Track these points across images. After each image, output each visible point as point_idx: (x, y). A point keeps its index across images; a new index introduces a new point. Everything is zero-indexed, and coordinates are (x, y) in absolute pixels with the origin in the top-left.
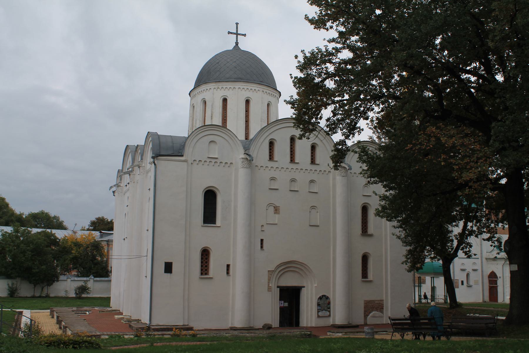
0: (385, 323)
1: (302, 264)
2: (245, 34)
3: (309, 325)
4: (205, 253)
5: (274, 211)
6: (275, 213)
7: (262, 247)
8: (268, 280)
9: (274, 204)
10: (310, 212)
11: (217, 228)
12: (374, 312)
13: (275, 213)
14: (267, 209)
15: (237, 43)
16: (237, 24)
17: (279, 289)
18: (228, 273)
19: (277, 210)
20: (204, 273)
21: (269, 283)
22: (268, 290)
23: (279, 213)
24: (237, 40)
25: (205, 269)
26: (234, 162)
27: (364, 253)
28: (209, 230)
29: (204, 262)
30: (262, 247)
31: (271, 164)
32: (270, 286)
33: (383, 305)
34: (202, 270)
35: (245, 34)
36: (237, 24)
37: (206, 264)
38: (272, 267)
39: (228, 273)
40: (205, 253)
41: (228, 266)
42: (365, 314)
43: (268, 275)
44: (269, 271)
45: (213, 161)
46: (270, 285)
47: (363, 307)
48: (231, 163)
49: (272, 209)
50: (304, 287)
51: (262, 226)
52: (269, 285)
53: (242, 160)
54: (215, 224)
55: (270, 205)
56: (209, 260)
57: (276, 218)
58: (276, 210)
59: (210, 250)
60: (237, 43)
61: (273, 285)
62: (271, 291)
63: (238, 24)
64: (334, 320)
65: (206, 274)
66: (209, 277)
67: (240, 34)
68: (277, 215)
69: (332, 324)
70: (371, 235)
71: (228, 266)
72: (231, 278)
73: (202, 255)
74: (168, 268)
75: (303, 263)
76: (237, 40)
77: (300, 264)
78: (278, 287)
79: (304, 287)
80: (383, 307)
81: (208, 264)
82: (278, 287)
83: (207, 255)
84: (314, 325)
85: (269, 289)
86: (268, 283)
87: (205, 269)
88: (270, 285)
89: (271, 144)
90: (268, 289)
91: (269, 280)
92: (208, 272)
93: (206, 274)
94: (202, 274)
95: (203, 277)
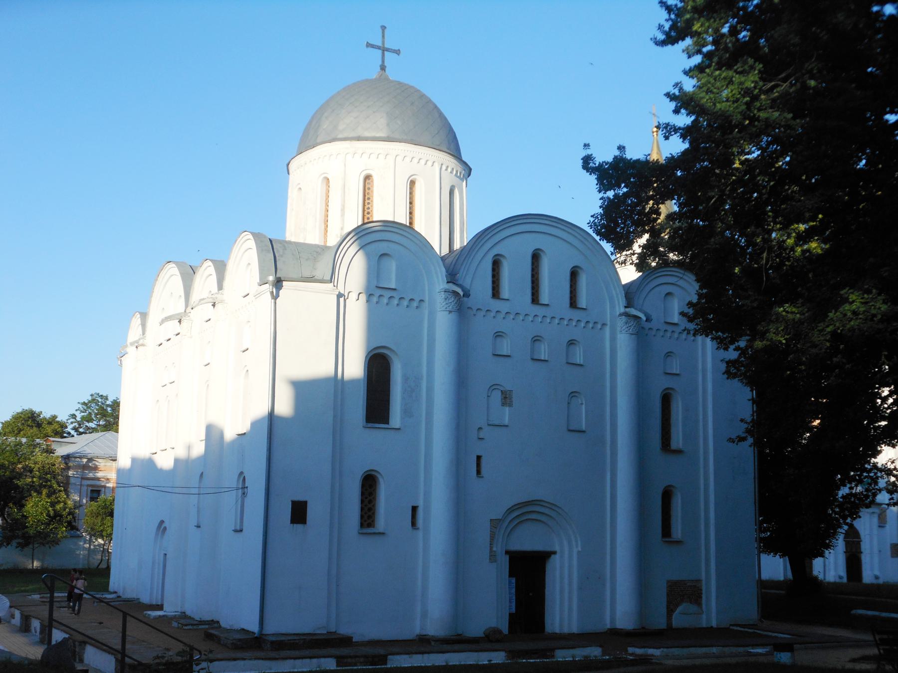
0: (704, 624)
1: (552, 506)
2: (399, 50)
3: (566, 630)
4: (369, 483)
5: (502, 399)
6: (503, 404)
7: (479, 472)
8: (490, 539)
9: (501, 385)
10: (568, 403)
11: (392, 432)
12: (684, 605)
13: (503, 404)
14: (488, 396)
15: (383, 68)
16: (383, 28)
17: (508, 557)
18: (414, 524)
19: (507, 398)
21: (492, 544)
22: (490, 559)
23: (510, 405)
24: (383, 61)
25: (368, 516)
26: (427, 299)
27: (669, 486)
28: (377, 436)
30: (479, 472)
31: (496, 305)
32: (495, 551)
33: (701, 590)
35: (399, 50)
36: (383, 28)
37: (370, 506)
38: (497, 513)
39: (414, 524)
40: (369, 483)
41: (414, 509)
42: (668, 607)
43: (491, 528)
44: (491, 520)
45: (388, 294)
46: (494, 549)
47: (666, 594)
48: (422, 301)
49: (497, 396)
50: (554, 553)
51: (480, 428)
52: (491, 548)
53: (443, 295)
54: (388, 423)
55: (493, 387)
56: (375, 498)
57: (506, 415)
58: (505, 398)
59: (378, 476)
60: (383, 68)
61: (499, 549)
62: (495, 561)
63: (385, 28)
64: (613, 619)
66: (377, 531)
67: (388, 50)
68: (507, 409)
69: (608, 629)
70: (679, 452)
72: (420, 534)
73: (363, 486)
74: (299, 512)
75: (556, 505)
76: (383, 61)
77: (551, 506)
78: (507, 552)
79: (554, 553)
80: (702, 594)
81: (374, 506)
82: (507, 552)
84: (575, 630)
85: (493, 557)
86: (490, 544)
87: (368, 516)
88: (494, 549)
89: (496, 264)
90: (491, 556)
91: (492, 538)
92: (373, 521)
94: (362, 525)
95: (365, 531)
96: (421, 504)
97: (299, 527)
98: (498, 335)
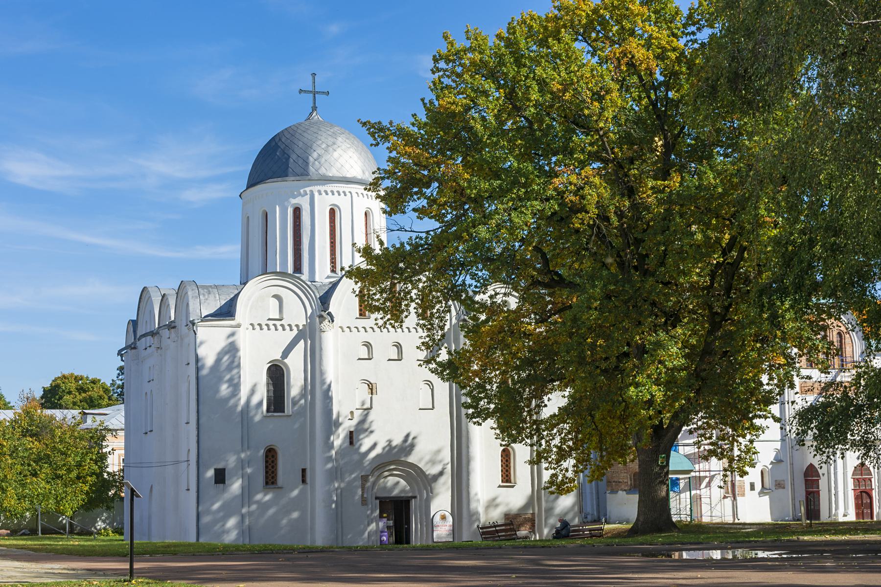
4: (271, 455)
17: (378, 501)
19: (372, 388)
20: (270, 482)
29: (270, 467)
34: (267, 478)
41: (304, 471)
54: (284, 412)
56: (276, 464)
62: (366, 504)
65: (274, 482)
71: (304, 471)
72: (309, 487)
73: (267, 456)
78: (377, 498)
79: (415, 497)
81: (276, 469)
83: (273, 456)
88: (365, 496)
93: (273, 483)
94: (267, 483)
96: (308, 467)
97: (221, 485)
98: (368, 345)
